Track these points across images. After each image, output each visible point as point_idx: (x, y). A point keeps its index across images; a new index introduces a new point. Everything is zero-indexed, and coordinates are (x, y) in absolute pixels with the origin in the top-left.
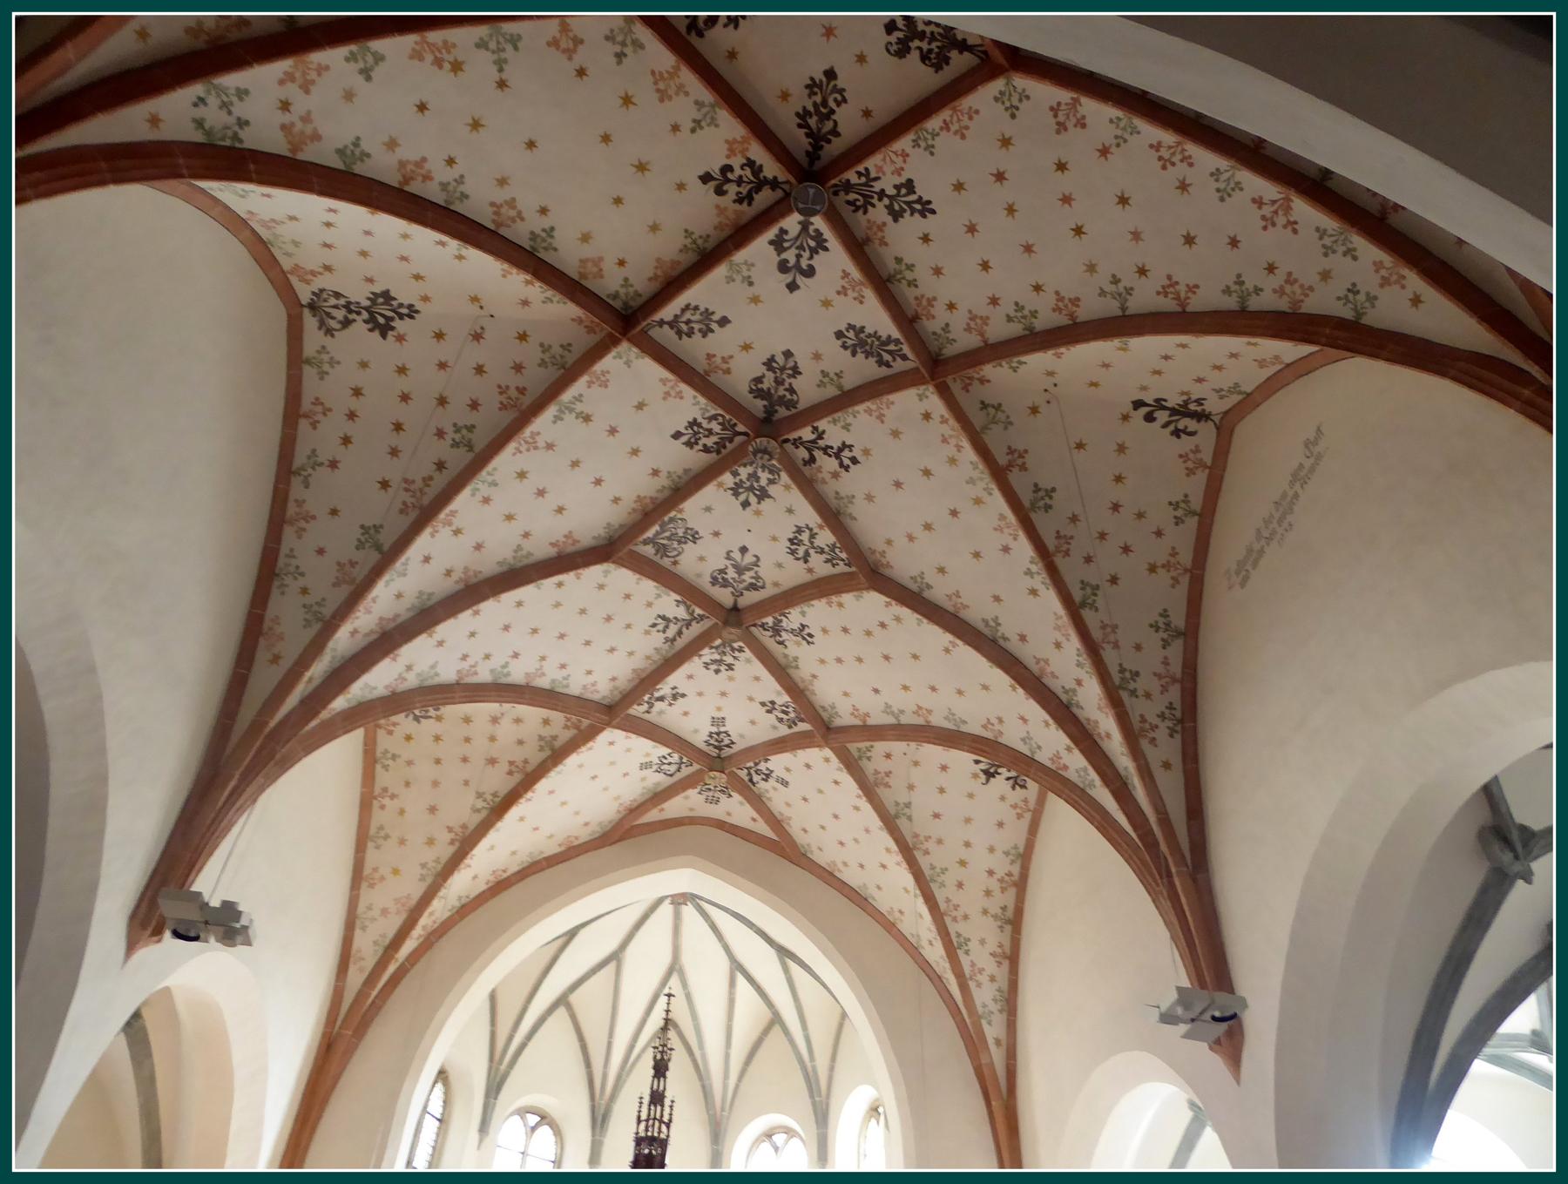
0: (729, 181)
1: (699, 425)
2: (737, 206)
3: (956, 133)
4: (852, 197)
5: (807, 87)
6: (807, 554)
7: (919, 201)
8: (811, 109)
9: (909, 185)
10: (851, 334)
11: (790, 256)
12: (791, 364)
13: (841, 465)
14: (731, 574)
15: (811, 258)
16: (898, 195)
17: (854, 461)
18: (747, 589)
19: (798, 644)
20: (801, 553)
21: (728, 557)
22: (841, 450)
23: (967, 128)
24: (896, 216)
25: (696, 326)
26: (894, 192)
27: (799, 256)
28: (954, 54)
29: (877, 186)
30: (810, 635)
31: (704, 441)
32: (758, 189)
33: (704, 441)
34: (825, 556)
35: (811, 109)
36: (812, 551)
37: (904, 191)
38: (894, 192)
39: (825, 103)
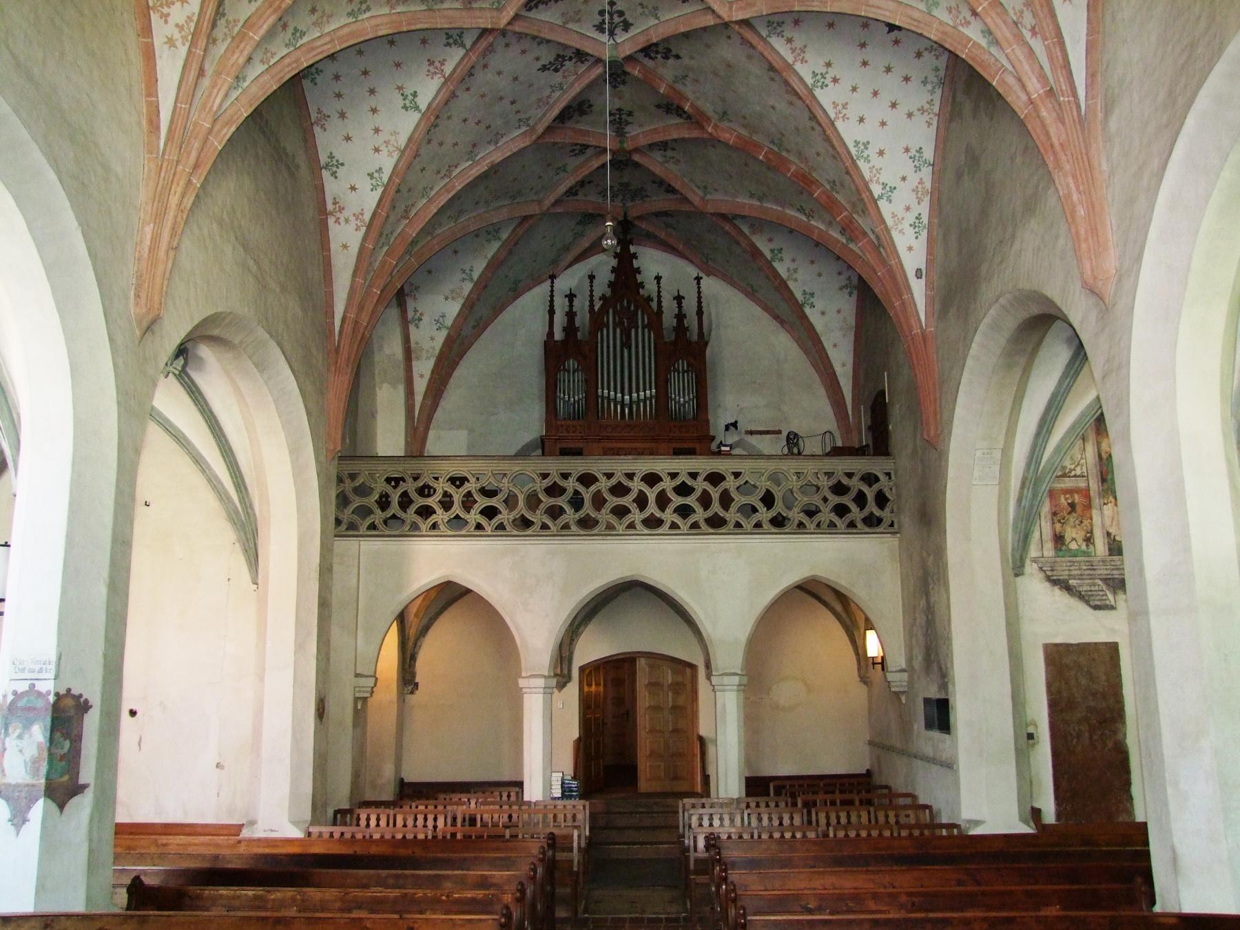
24: (558, 56)
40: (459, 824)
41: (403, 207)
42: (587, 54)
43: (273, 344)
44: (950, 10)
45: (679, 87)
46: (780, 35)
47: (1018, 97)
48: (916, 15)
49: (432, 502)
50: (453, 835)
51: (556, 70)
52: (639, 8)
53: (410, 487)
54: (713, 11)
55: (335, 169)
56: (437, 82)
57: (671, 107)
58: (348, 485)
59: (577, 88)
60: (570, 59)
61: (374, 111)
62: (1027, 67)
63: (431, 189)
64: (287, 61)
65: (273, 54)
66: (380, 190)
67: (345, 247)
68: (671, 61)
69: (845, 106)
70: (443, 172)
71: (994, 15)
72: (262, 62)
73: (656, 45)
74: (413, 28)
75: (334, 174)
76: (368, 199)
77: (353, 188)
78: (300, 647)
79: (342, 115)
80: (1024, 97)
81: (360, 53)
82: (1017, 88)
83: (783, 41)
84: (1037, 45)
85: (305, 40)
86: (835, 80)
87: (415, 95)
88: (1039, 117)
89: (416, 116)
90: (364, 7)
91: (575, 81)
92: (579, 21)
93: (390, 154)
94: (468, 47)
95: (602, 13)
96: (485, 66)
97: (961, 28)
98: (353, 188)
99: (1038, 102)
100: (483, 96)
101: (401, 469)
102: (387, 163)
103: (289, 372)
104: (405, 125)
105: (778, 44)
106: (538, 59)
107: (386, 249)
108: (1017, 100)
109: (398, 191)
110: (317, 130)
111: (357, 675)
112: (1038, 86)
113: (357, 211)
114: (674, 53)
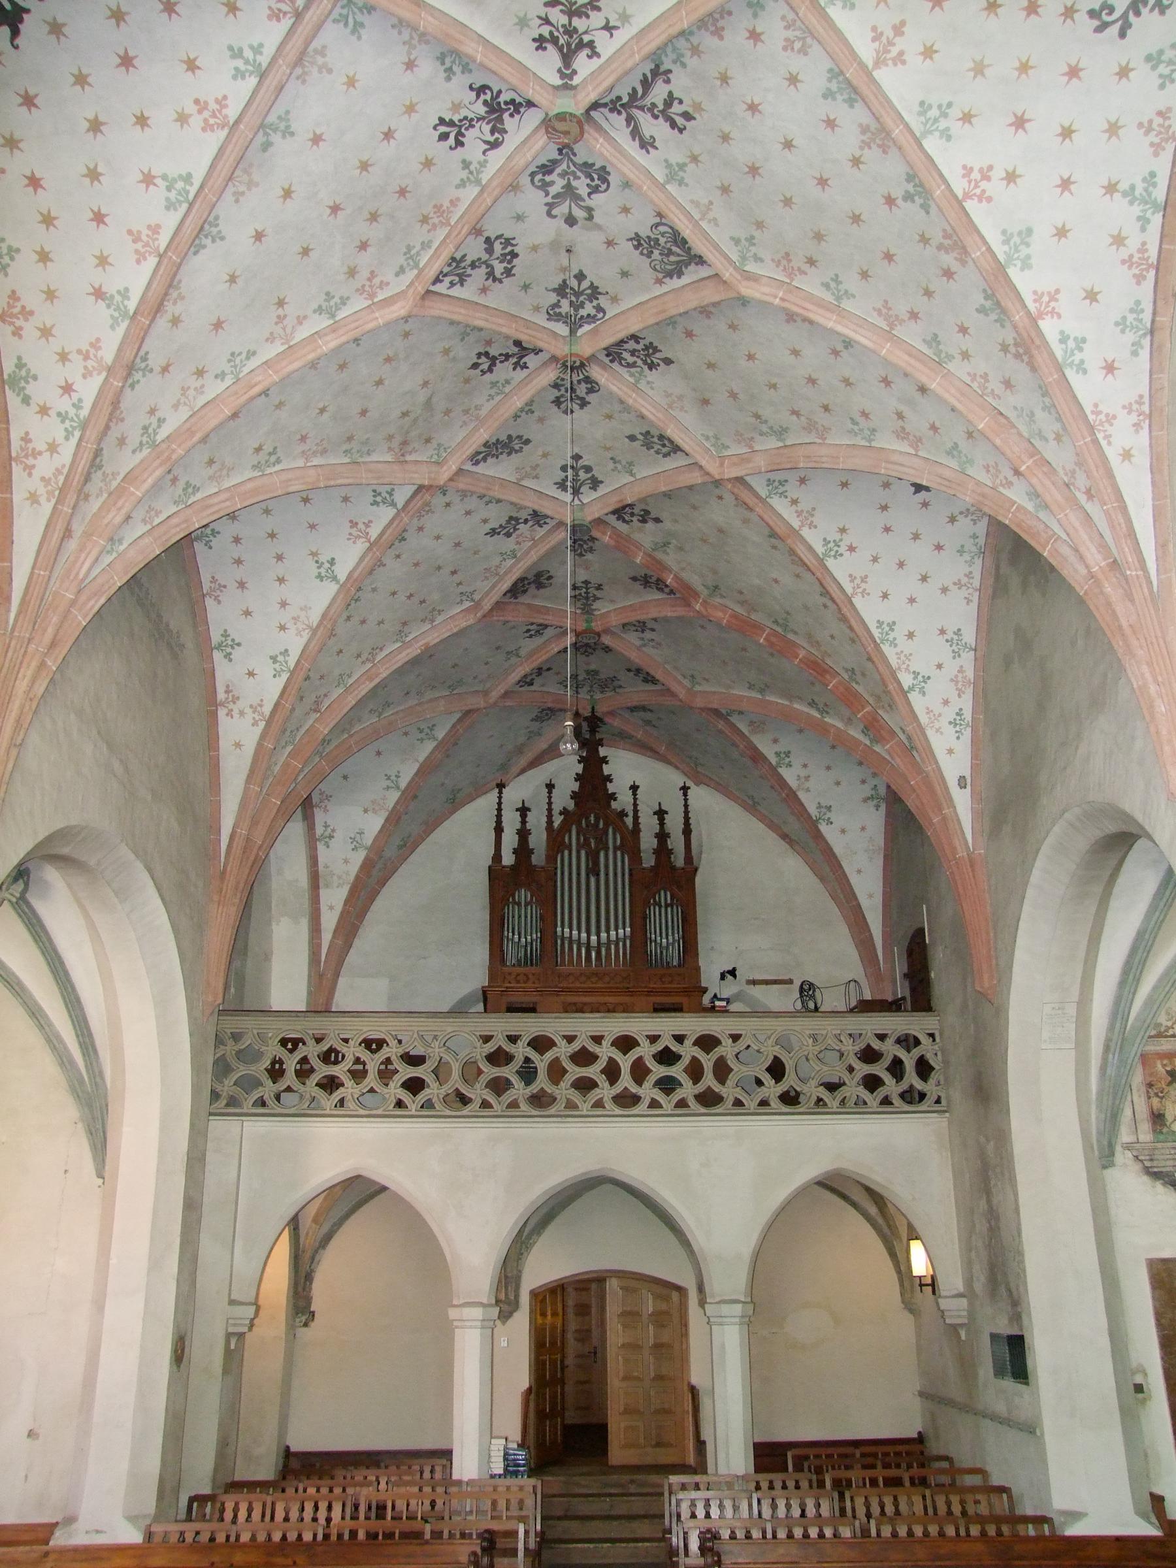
1: (645, 362)
6: (490, 250)
7: (499, 534)
10: (517, 447)
12: (563, 406)
13: (487, 354)
14: (581, 185)
17: (475, 366)
18: (555, 163)
19: (456, 107)
20: (498, 248)
21: (589, 210)
22: (493, 364)
24: (511, 518)
25: (655, 440)
29: (530, 523)
30: (444, 137)
31: (640, 347)
33: (640, 347)
34: (469, 259)
36: (485, 257)
40: (362, 1516)
41: (314, 699)
42: (547, 517)
43: (139, 866)
44: (987, 468)
45: (660, 555)
46: (783, 495)
47: (1076, 570)
48: (947, 473)
49: (339, 1071)
50: (353, 1534)
51: (508, 535)
53: (311, 1050)
54: (701, 467)
55: (229, 650)
56: (361, 546)
57: (650, 580)
58: (230, 1048)
59: (534, 556)
61: (281, 580)
62: (1085, 537)
63: (349, 676)
64: (175, 521)
65: (158, 513)
66: (285, 676)
67: (238, 745)
68: (650, 525)
69: (864, 579)
70: (364, 657)
71: (1040, 475)
72: (144, 521)
73: (631, 506)
74: (332, 483)
75: (228, 656)
76: (268, 688)
77: (251, 674)
78: (155, 1264)
79: (242, 585)
80: (1083, 571)
81: (267, 512)
82: (1073, 559)
83: (786, 502)
84: (1093, 509)
85: (199, 496)
86: (851, 549)
87: (332, 562)
88: (1102, 593)
89: (334, 587)
90: (273, 459)
91: (530, 548)
92: (536, 477)
93: (299, 634)
94: (400, 506)
95: (564, 468)
96: (421, 529)
97: (1001, 489)
98: (251, 674)
99: (1100, 576)
100: (416, 565)
101: (299, 1027)
102: (295, 643)
103: (159, 901)
104: (319, 598)
105: (780, 505)
106: (485, 521)
107: (289, 748)
108: (1074, 572)
109: (307, 678)
110: (209, 602)
111: (232, 1302)
112: (1098, 557)
113: (255, 702)
114: (653, 515)
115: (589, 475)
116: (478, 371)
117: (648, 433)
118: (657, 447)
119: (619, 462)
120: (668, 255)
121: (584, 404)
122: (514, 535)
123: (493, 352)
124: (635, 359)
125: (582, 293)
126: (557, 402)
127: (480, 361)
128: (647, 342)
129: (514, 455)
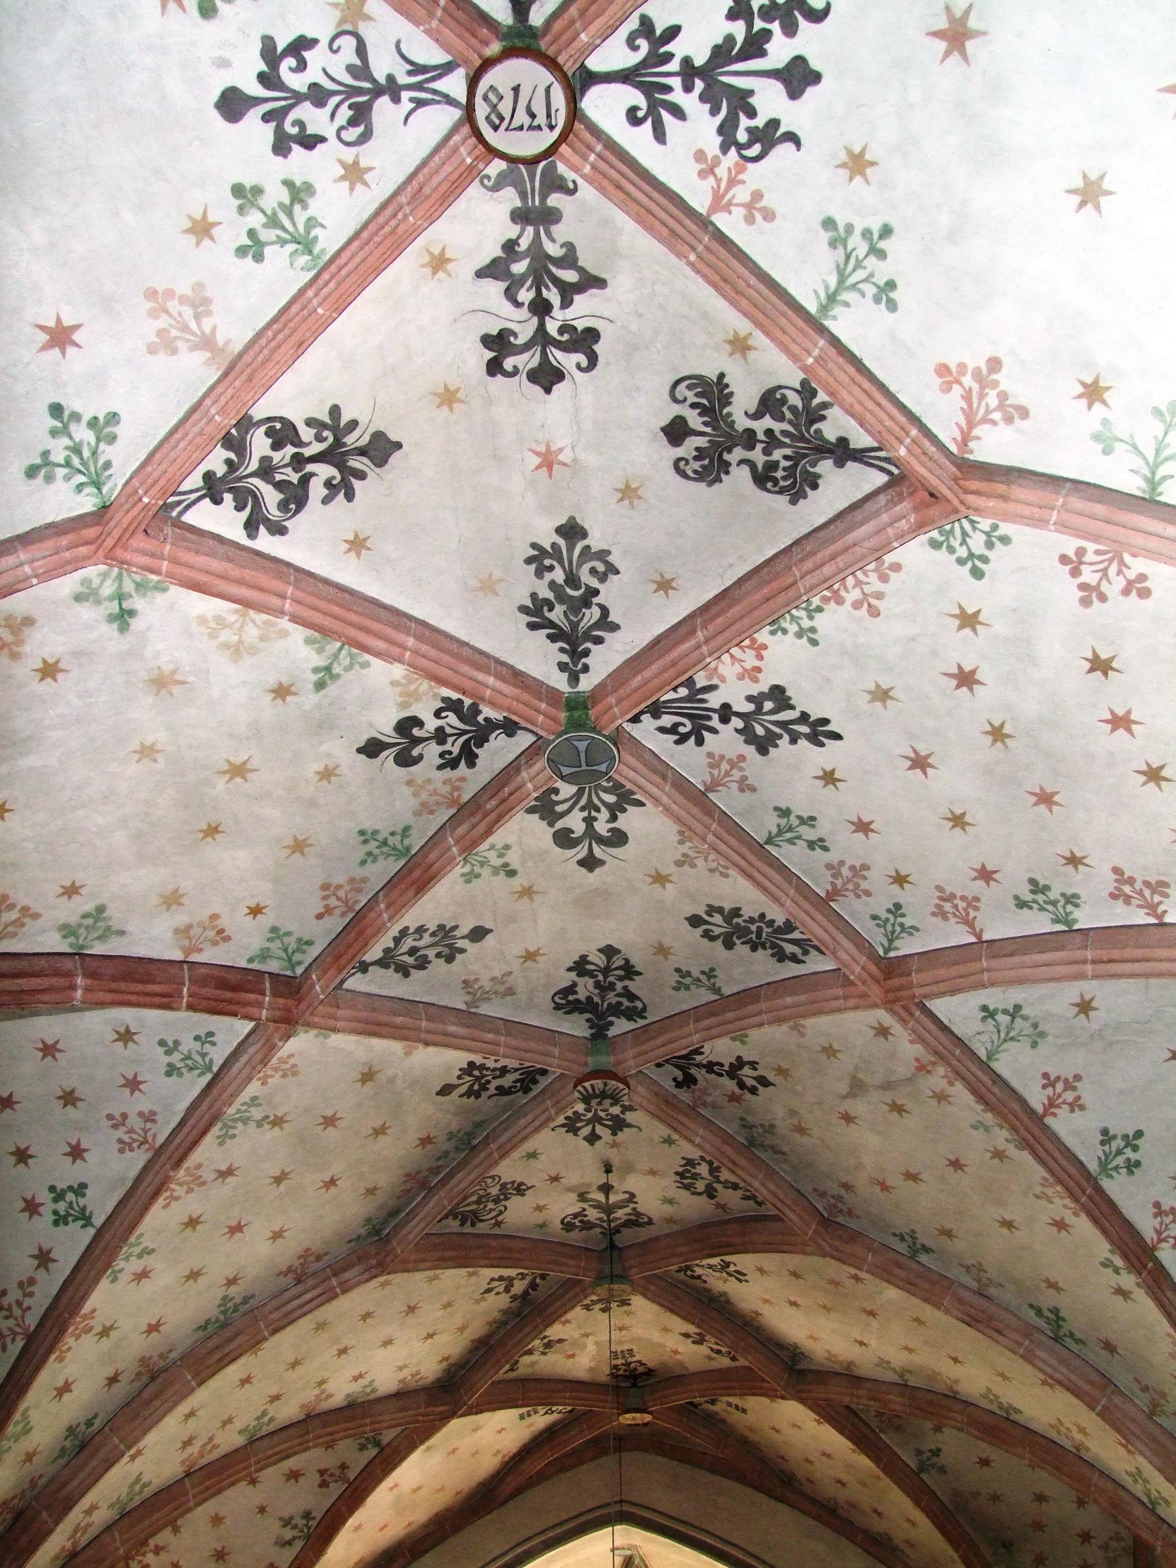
0: (418, 741)
2: (447, 773)
3: (857, 605)
4: (667, 720)
5: (529, 561)
7: (804, 718)
8: (550, 595)
9: (778, 694)
10: (718, 919)
11: (575, 822)
13: (742, 1085)
15: (614, 818)
16: (759, 709)
17: (764, 1082)
20: (700, 1186)
23: (879, 596)
24: (764, 745)
25: (431, 953)
26: (750, 707)
27: (589, 821)
28: (825, 467)
29: (714, 700)
32: (481, 740)
35: (550, 595)
37: (768, 705)
38: (750, 707)
39: (572, 580)
52: (515, 864)
60: (726, 712)
68: (384, 724)
83: (154, 1128)
95: (619, 838)
96: (986, 875)
114: (388, 755)
115: (560, 825)
116: (760, 1072)
117: (450, 959)
118: (427, 939)
119: (496, 871)
120: (480, 1197)
121: (581, 966)
122: (763, 686)
123: (730, 1085)
124: (499, 1065)
125: (589, 1122)
126: (629, 971)
127: (754, 1083)
128: (485, 1095)
129: (728, 906)
